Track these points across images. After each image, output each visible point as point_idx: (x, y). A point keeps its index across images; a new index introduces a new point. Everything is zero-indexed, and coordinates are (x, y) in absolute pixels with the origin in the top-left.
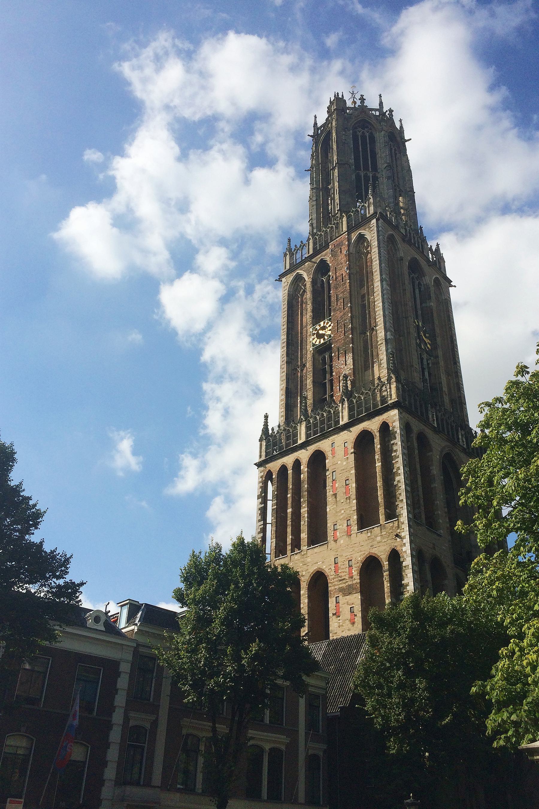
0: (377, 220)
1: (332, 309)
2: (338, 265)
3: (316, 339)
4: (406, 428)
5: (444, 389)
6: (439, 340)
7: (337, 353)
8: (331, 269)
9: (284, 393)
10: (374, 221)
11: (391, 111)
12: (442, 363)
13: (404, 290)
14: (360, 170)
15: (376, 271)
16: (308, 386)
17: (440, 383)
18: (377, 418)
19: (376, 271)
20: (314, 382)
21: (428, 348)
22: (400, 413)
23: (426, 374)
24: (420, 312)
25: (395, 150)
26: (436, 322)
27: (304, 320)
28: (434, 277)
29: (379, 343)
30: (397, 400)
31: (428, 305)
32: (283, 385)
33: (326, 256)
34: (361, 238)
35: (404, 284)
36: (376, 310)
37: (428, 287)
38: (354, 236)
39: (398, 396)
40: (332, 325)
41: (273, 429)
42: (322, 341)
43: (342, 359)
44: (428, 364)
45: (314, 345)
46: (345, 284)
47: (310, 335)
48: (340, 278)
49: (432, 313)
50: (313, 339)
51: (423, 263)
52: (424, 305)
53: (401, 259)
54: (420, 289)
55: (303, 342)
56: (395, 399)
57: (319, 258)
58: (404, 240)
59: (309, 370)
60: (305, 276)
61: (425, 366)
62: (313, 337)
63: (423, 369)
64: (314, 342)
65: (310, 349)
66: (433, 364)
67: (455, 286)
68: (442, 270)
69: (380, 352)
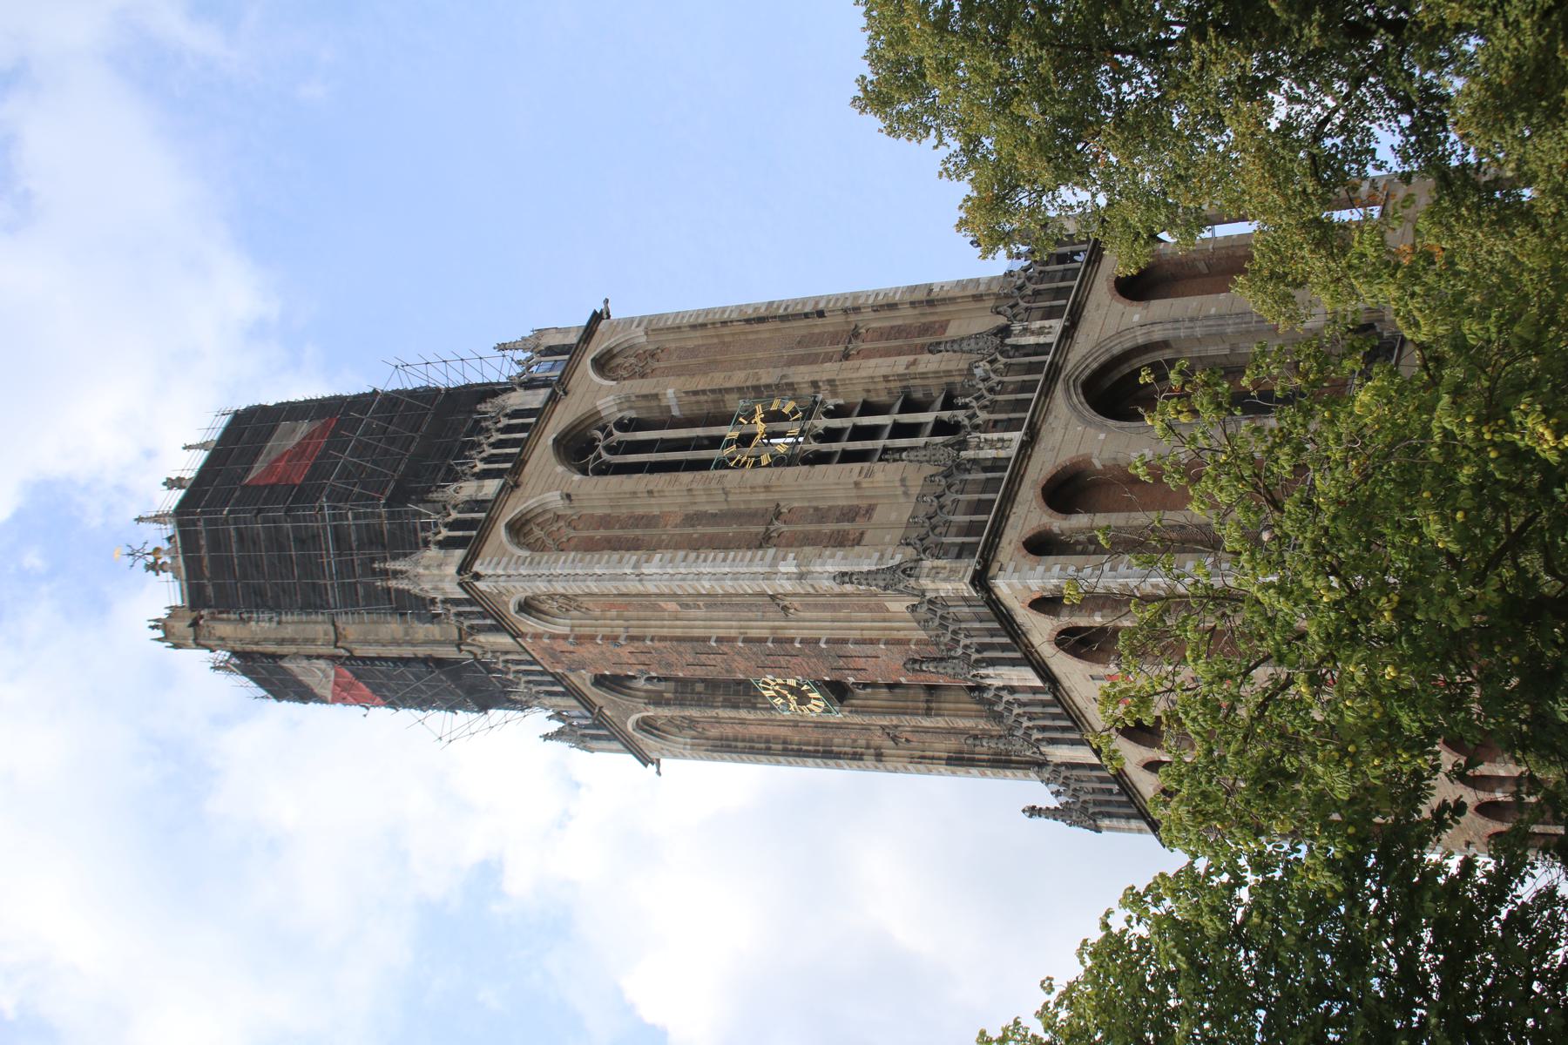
0: (477, 577)
5: (901, 370)
6: (768, 377)
11: (171, 484)
13: (650, 492)
17: (886, 378)
20: (928, 712)
26: (718, 380)
28: (591, 373)
43: (861, 663)
65: (838, 716)
66: (834, 394)
67: (607, 301)
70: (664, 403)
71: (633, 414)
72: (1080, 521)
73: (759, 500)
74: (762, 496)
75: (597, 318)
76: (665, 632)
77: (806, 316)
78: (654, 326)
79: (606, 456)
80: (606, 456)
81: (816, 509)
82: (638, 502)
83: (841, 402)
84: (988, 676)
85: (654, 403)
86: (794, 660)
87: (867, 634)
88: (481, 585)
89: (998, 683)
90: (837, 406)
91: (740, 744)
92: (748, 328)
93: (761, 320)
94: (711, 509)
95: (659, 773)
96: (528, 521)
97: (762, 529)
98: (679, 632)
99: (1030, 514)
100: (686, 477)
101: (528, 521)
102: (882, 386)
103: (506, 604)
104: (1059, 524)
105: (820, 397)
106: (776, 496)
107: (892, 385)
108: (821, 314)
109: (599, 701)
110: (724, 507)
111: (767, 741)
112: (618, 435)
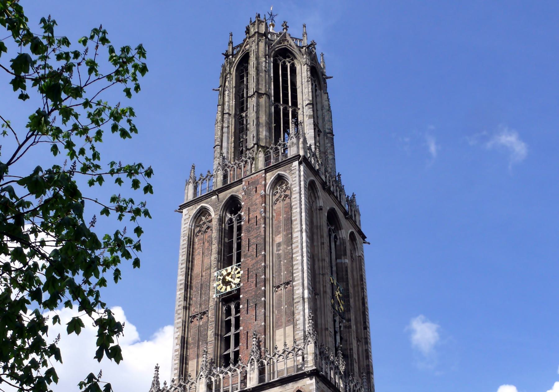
0: (300, 163)
1: (242, 254)
2: (252, 205)
3: (221, 285)
5: (354, 356)
7: (246, 306)
8: (244, 209)
9: (179, 342)
10: (296, 163)
12: (354, 327)
13: (323, 243)
14: (280, 102)
15: (296, 220)
16: (209, 338)
17: (351, 349)
18: (291, 385)
19: (296, 220)
20: (216, 335)
21: (341, 310)
22: (317, 382)
23: (338, 338)
24: (334, 269)
25: (316, 85)
26: (350, 282)
27: (206, 261)
28: (350, 231)
29: (295, 301)
30: (314, 368)
31: (343, 261)
32: (179, 333)
33: (238, 191)
34: (280, 180)
35: (322, 237)
36: (294, 263)
37: (343, 242)
38: (271, 177)
39: (316, 364)
40: (242, 272)
41: (165, 384)
42: (229, 289)
43: (252, 313)
44: (340, 327)
45: (218, 292)
46: (259, 227)
47: (214, 280)
48: (253, 221)
49: (347, 271)
50: (218, 285)
51: (340, 215)
52: (338, 261)
53: (321, 209)
54: (335, 242)
55: (205, 286)
56: (312, 366)
57: (230, 193)
58: (324, 189)
59: (210, 319)
60: (211, 210)
61: (338, 330)
62: (217, 283)
63: (335, 332)
64: (218, 288)
66: (345, 327)
67: (369, 243)
68: (358, 224)
69: (296, 312)
70: (343, 257)
71: (338, 243)
74: (322, 289)
75: (364, 237)
77: (365, 322)
78: (361, 259)
82: (319, 237)
84: (251, 365)
85: (342, 253)
86: (253, 285)
87: (268, 318)
88: (296, 163)
89: (248, 369)
92: (360, 298)
94: (316, 266)
98: (267, 239)
103: (285, 171)
105: (344, 321)
107: (349, 351)
109: (221, 195)
110: (317, 272)
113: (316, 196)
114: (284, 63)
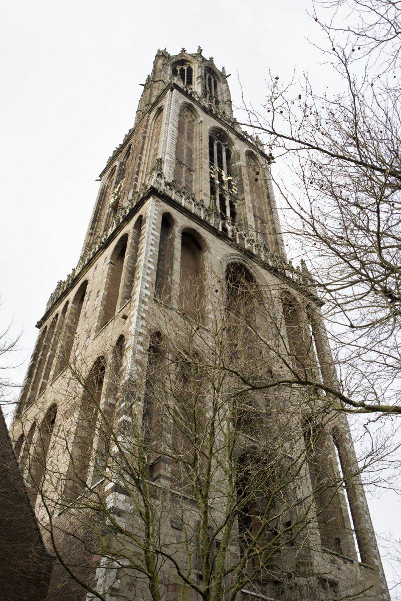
4: (167, 222)
5: (249, 223)
66: (239, 206)
72: (178, 243)
73: (196, 167)
76: (146, 145)
79: (216, 142)
80: (216, 142)
81: (192, 181)
83: (236, 207)
90: (234, 206)
91: (103, 198)
93: (269, 197)
95: (96, 180)
96: (192, 112)
97: (184, 162)
99: (181, 222)
100: (207, 151)
101: (192, 112)
102: (243, 218)
104: (177, 231)
106: (198, 171)
108: (271, 213)
111: (103, 204)
112: (224, 149)
113: (197, 115)
114: (182, 68)
